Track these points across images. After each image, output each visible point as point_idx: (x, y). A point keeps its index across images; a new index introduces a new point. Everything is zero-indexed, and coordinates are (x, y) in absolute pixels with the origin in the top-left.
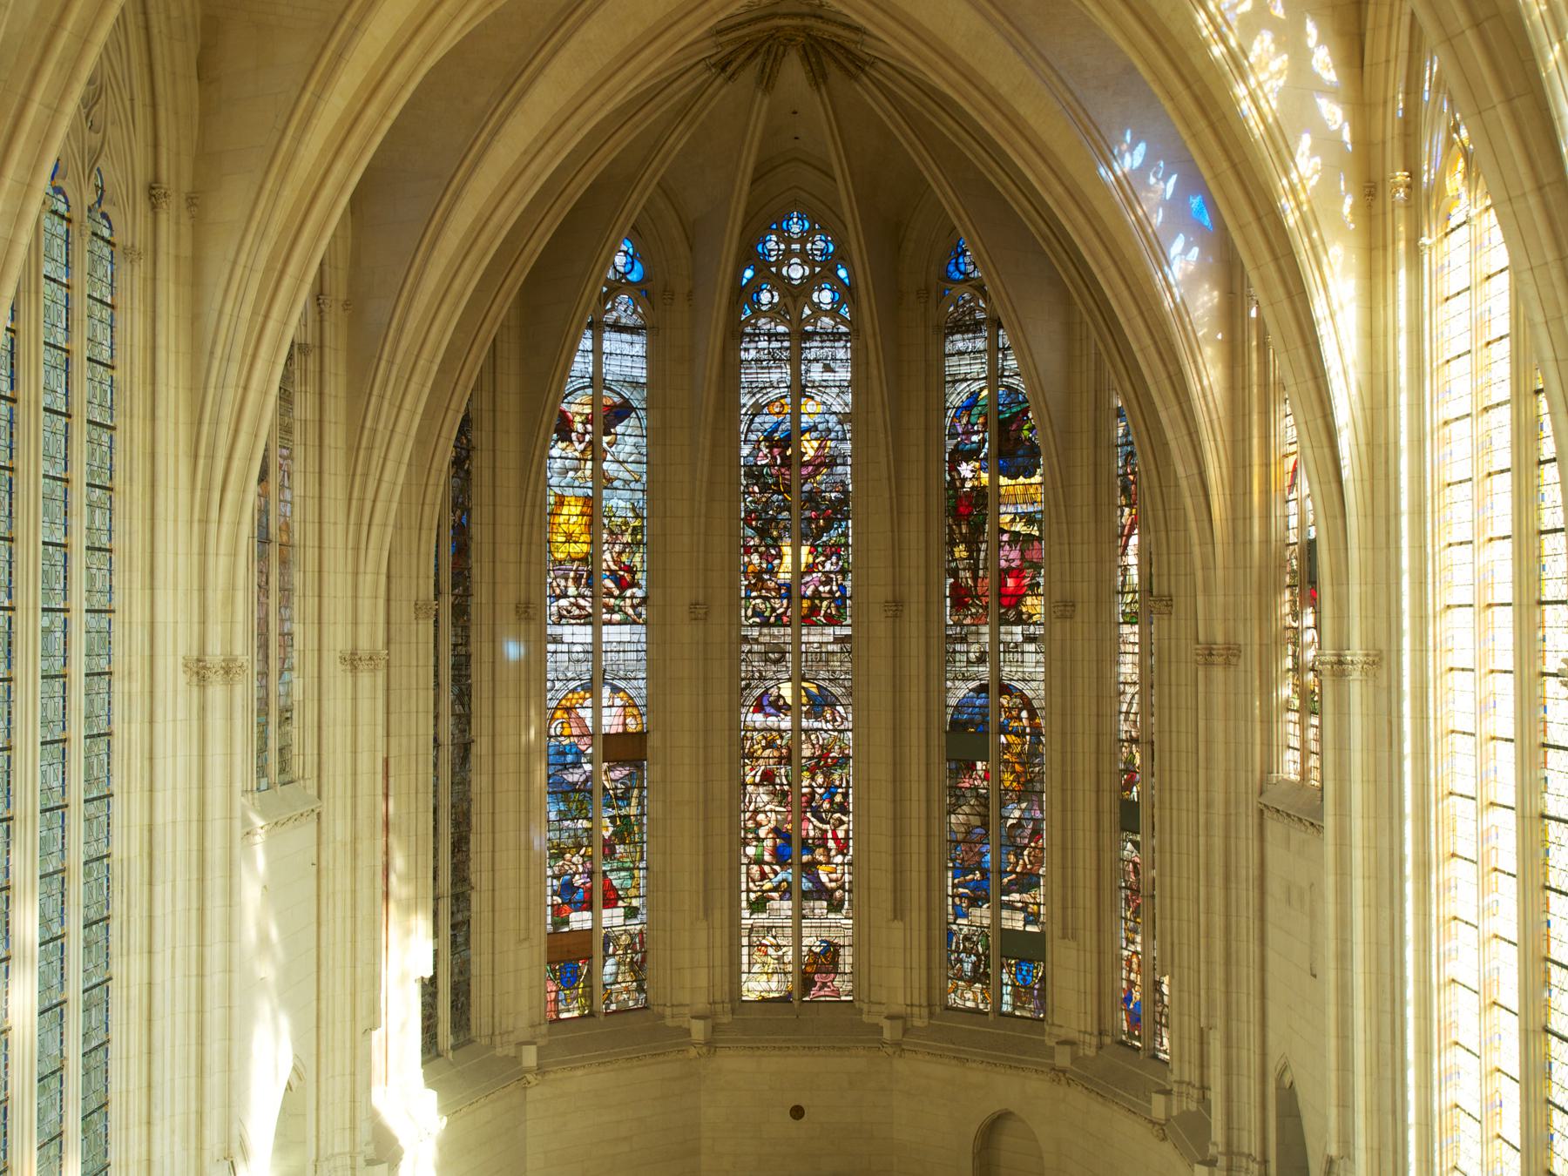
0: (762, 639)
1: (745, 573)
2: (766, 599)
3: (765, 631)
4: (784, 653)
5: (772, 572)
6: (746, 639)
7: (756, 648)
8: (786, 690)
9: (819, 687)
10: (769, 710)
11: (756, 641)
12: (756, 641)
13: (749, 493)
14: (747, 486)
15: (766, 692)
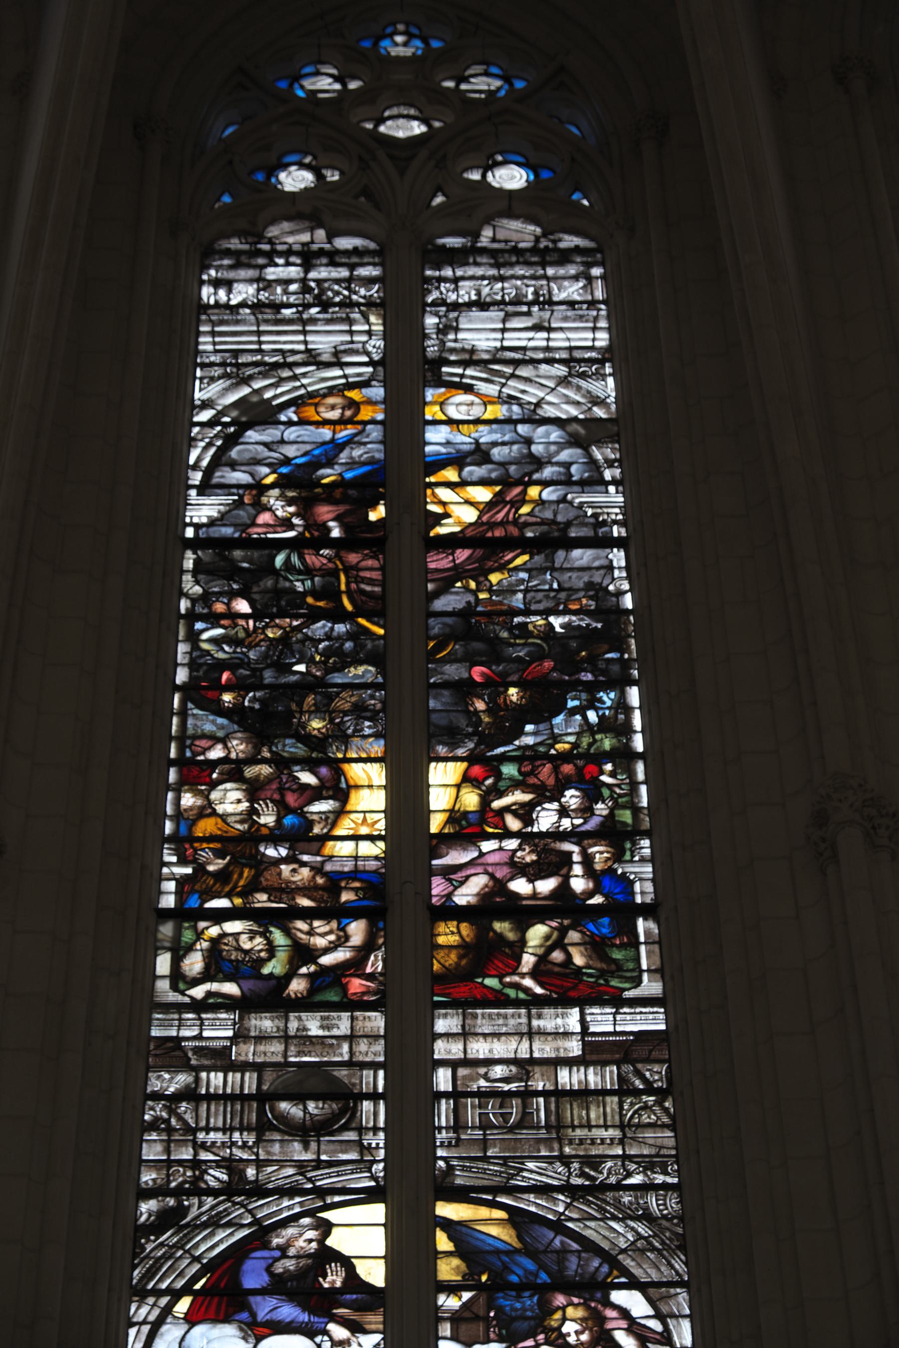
0: (247, 1052)
1: (184, 844)
2: (263, 919)
3: (266, 1023)
4: (348, 1099)
5: (302, 838)
6: (173, 1054)
7: (216, 1079)
8: (361, 1236)
9: (518, 1219)
10: (266, 1307)
11: (220, 1059)
12: (220, 1059)
13: (214, 620)
14: (206, 598)
15: (262, 1234)
